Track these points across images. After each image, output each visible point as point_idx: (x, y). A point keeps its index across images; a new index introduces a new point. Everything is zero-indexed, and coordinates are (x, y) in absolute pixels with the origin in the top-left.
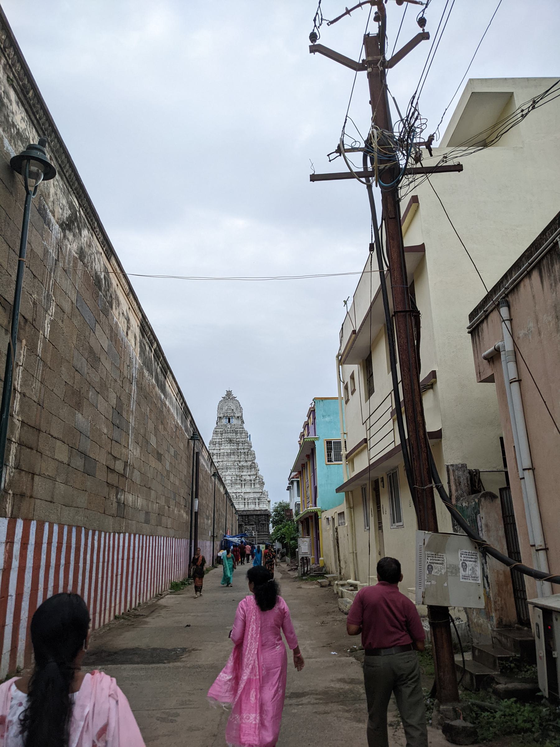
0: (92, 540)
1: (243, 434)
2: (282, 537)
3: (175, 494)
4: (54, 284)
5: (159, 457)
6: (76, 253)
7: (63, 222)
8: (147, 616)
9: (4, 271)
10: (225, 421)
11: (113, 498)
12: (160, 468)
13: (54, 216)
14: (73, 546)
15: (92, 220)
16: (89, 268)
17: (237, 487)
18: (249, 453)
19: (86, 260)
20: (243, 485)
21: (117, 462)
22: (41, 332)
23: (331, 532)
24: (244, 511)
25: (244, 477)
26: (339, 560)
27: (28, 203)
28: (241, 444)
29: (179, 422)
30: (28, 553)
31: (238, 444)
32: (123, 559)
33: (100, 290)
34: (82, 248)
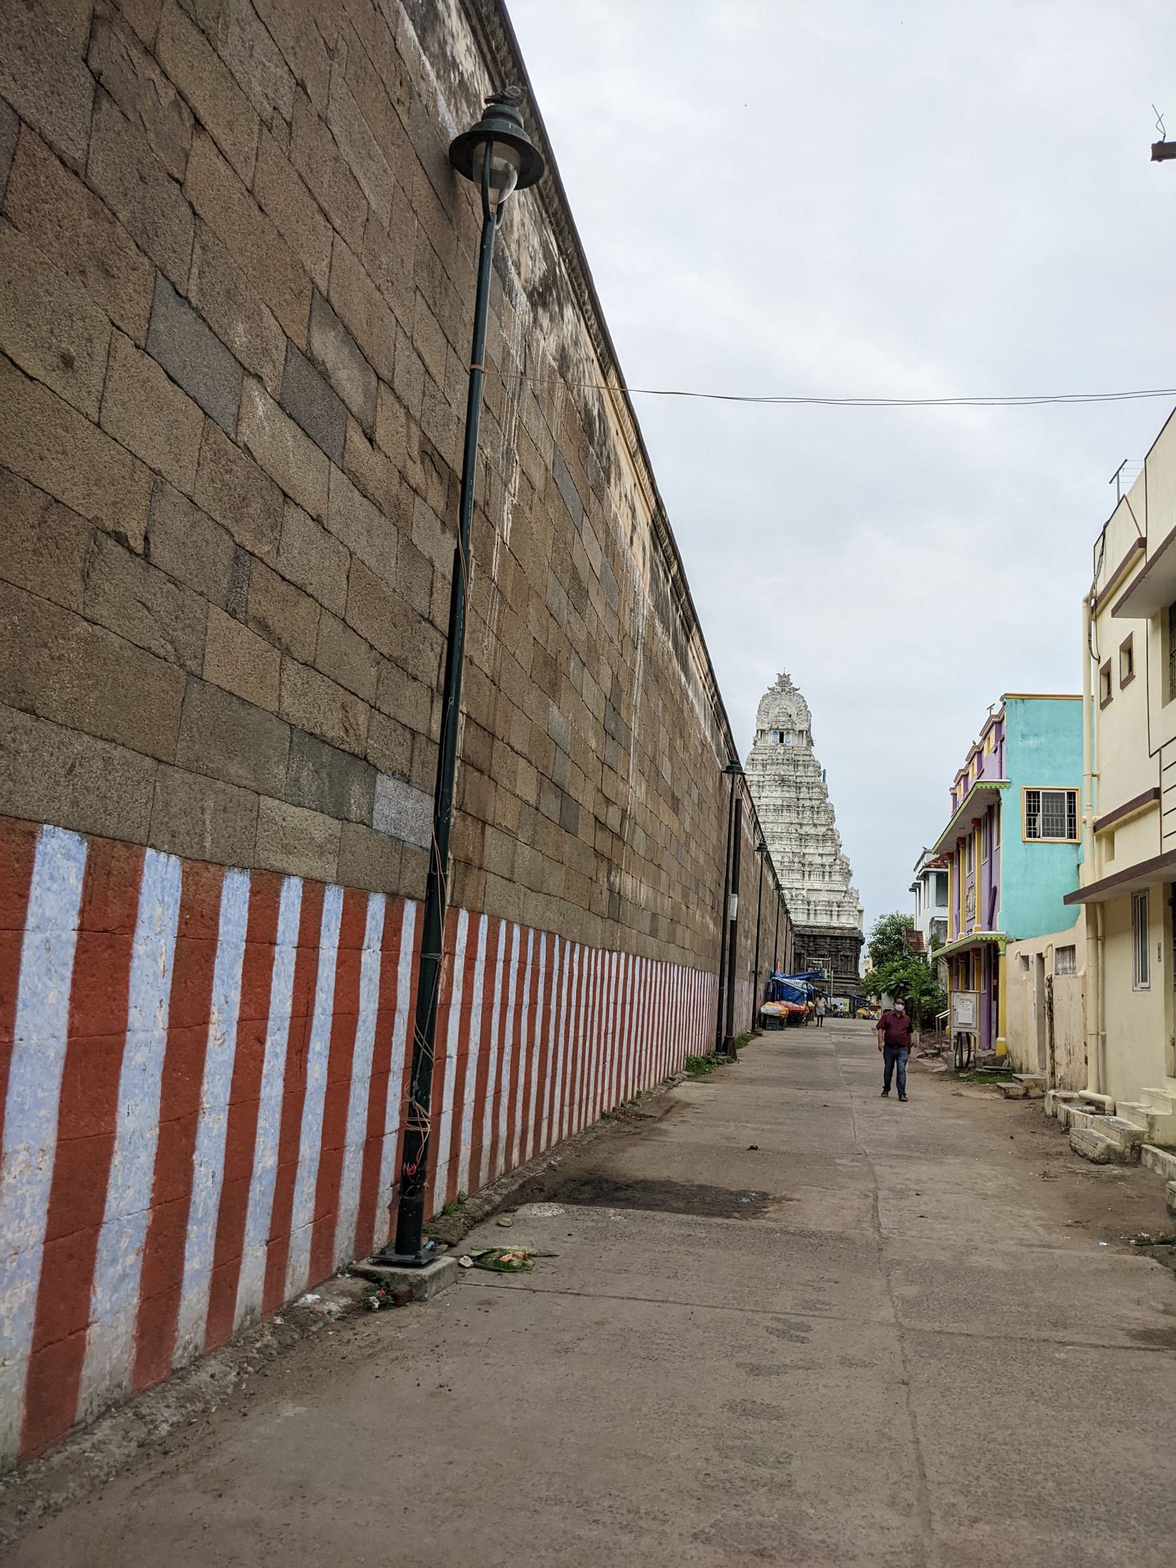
0: (570, 961)
1: (811, 768)
2: (898, 986)
3: (697, 881)
4: (518, 427)
5: (675, 805)
6: (554, 359)
7: (535, 288)
8: (660, 1120)
9: (439, 395)
10: (772, 739)
11: (603, 880)
12: (675, 826)
13: (519, 274)
14: (543, 970)
15: (580, 285)
16: (575, 392)
18: (822, 808)
19: (569, 376)
20: (807, 874)
21: (610, 809)
22: (498, 531)
23: (1033, 987)
26: (1052, 1047)
27: (487, 241)
29: (708, 734)
30: (476, 977)
32: (615, 1003)
33: (591, 441)
34: (563, 348)
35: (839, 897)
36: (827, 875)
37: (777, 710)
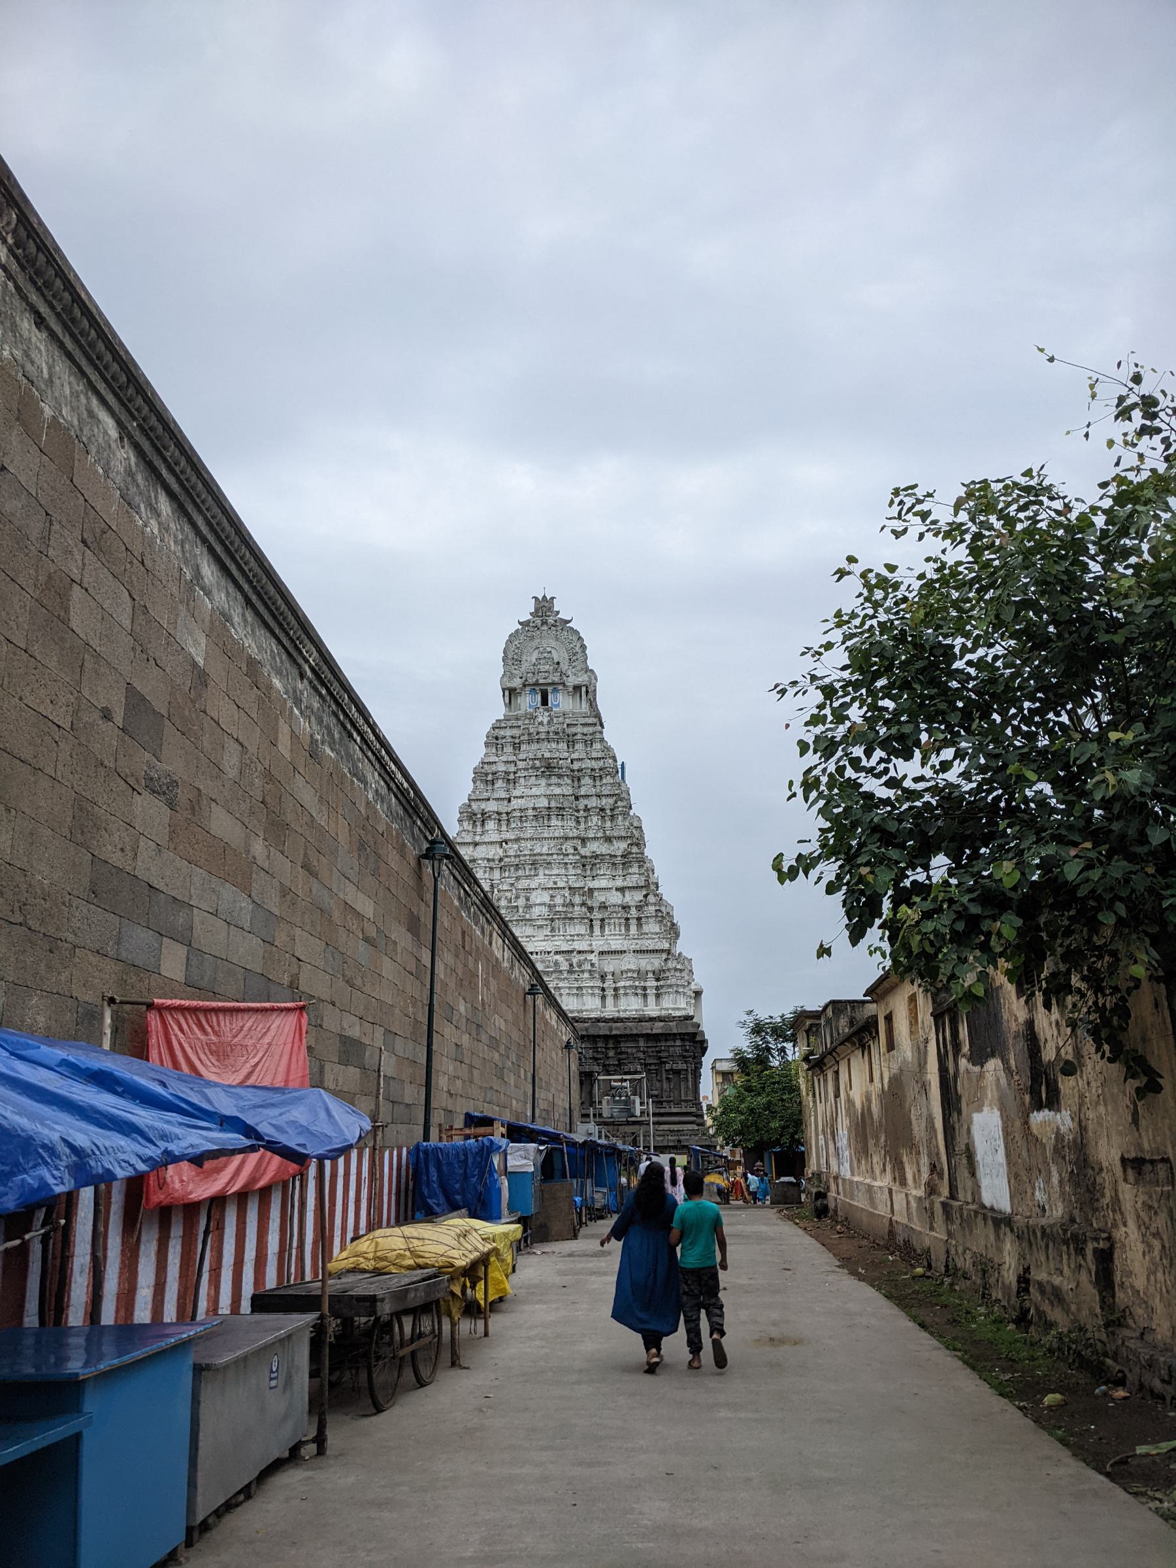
1: (597, 746)
10: (527, 702)
18: (618, 805)
20: (597, 924)
24: (598, 1020)
28: (586, 780)
31: (576, 778)
35: (656, 962)
36: (633, 922)
37: (535, 655)
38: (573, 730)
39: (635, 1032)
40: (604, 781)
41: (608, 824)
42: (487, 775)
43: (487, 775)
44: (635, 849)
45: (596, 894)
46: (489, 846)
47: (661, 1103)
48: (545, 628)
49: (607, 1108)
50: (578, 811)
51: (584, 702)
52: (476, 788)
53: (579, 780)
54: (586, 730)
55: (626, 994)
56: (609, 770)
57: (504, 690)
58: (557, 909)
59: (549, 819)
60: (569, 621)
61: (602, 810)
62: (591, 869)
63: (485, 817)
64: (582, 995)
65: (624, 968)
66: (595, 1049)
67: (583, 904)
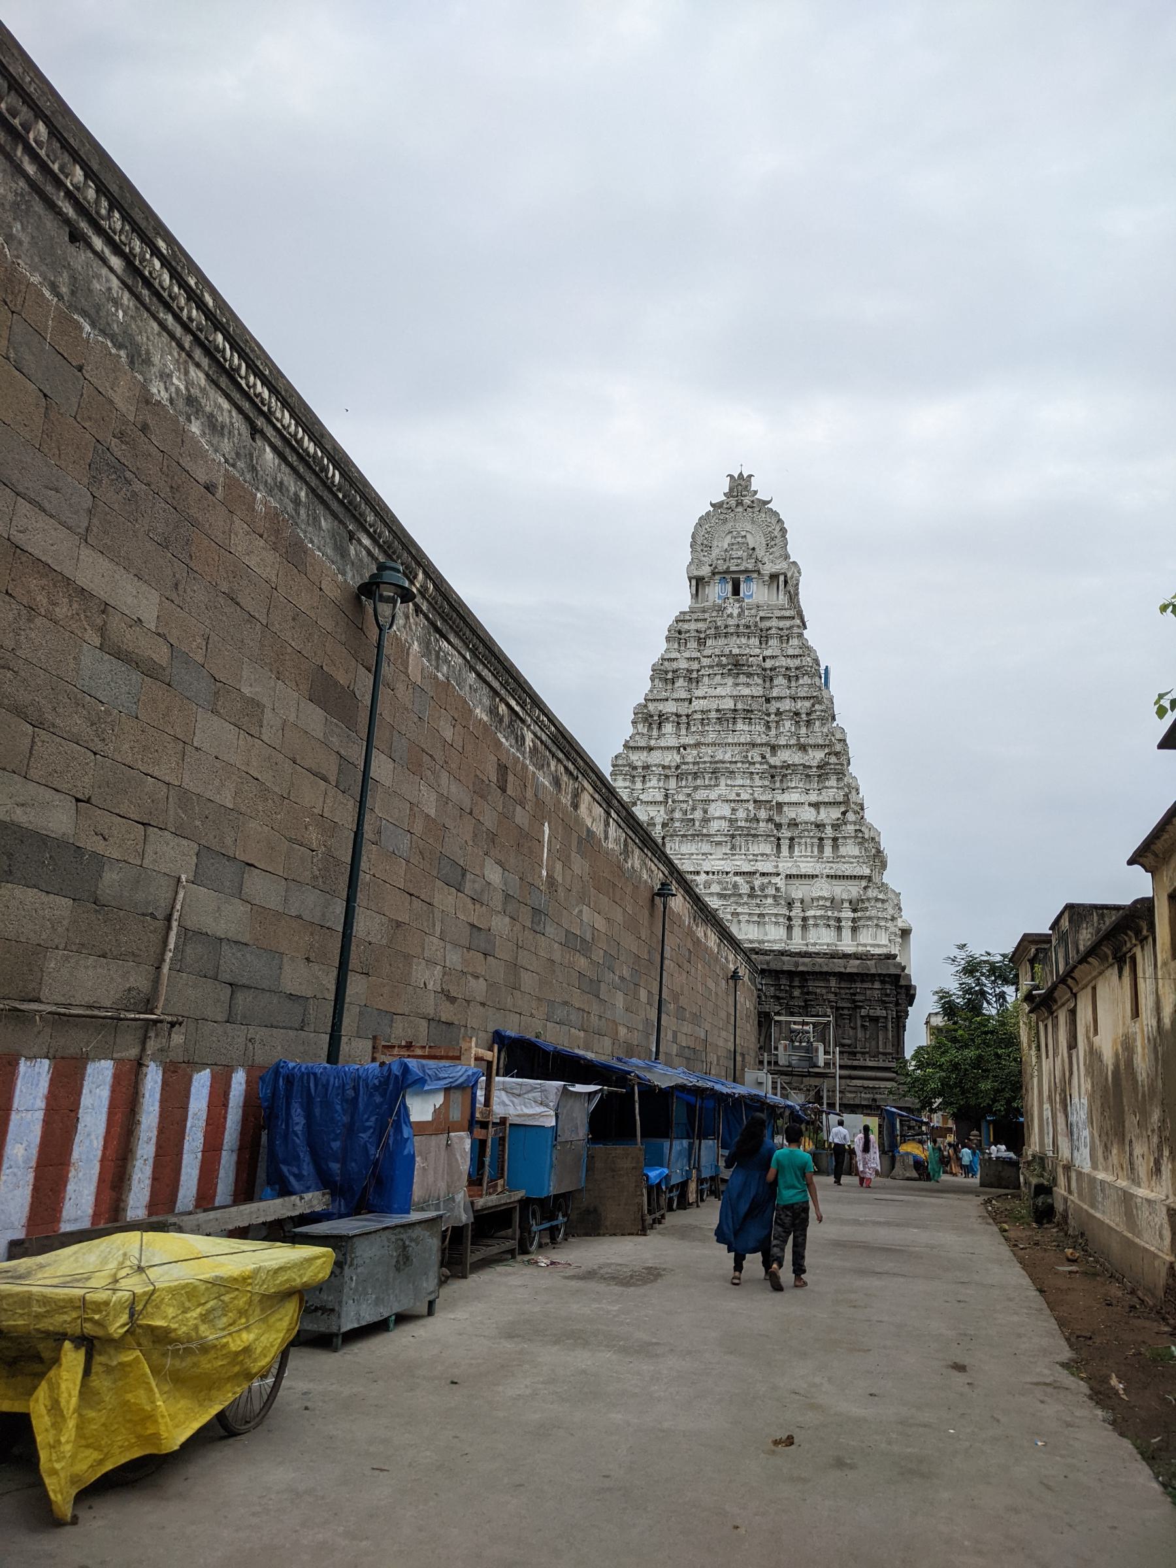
1: (794, 642)
10: (716, 592)
17: (755, 849)
18: (818, 710)
20: (785, 844)
24: (782, 953)
25: (790, 813)
28: (780, 680)
31: (768, 677)
35: (854, 890)
36: (828, 844)
37: (728, 540)
38: (767, 624)
39: (825, 969)
40: (801, 682)
41: (803, 730)
42: (666, 672)
43: (666, 672)
44: (833, 760)
45: (785, 809)
46: (666, 753)
47: (854, 1054)
48: (740, 509)
49: (783, 1054)
50: (769, 715)
51: (781, 593)
52: (653, 687)
53: (771, 680)
54: (782, 624)
55: (816, 925)
56: (809, 671)
57: (690, 579)
58: (739, 824)
59: (734, 723)
60: (769, 502)
61: (797, 714)
62: (781, 781)
63: (662, 718)
64: (764, 924)
65: (815, 895)
66: (778, 987)
67: (770, 820)
